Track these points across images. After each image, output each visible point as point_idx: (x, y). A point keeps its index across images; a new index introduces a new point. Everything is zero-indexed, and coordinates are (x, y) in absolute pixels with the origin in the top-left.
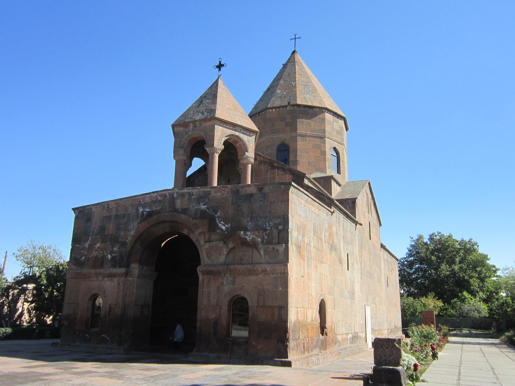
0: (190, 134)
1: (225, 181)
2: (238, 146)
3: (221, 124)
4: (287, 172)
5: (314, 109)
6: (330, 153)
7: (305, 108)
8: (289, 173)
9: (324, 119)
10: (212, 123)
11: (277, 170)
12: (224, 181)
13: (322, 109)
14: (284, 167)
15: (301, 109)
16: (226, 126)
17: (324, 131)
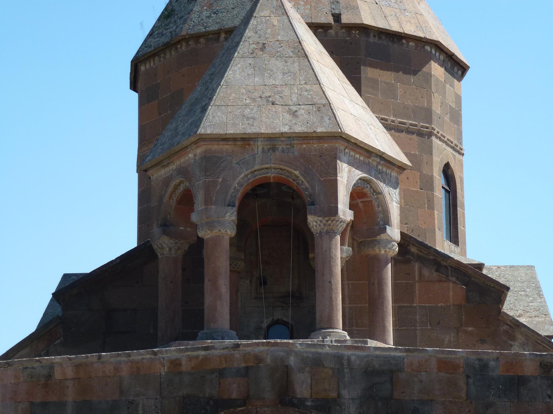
0: (257, 167)
1: (251, 281)
2: (361, 205)
3: (346, 151)
4: (447, 276)
5: (404, 41)
6: (439, 180)
7: (380, 38)
8: (454, 279)
9: (429, 75)
10: (326, 145)
11: (417, 266)
12: (248, 282)
13: (423, 43)
14: (439, 259)
15: (372, 39)
16: (353, 154)
17: (428, 114)
